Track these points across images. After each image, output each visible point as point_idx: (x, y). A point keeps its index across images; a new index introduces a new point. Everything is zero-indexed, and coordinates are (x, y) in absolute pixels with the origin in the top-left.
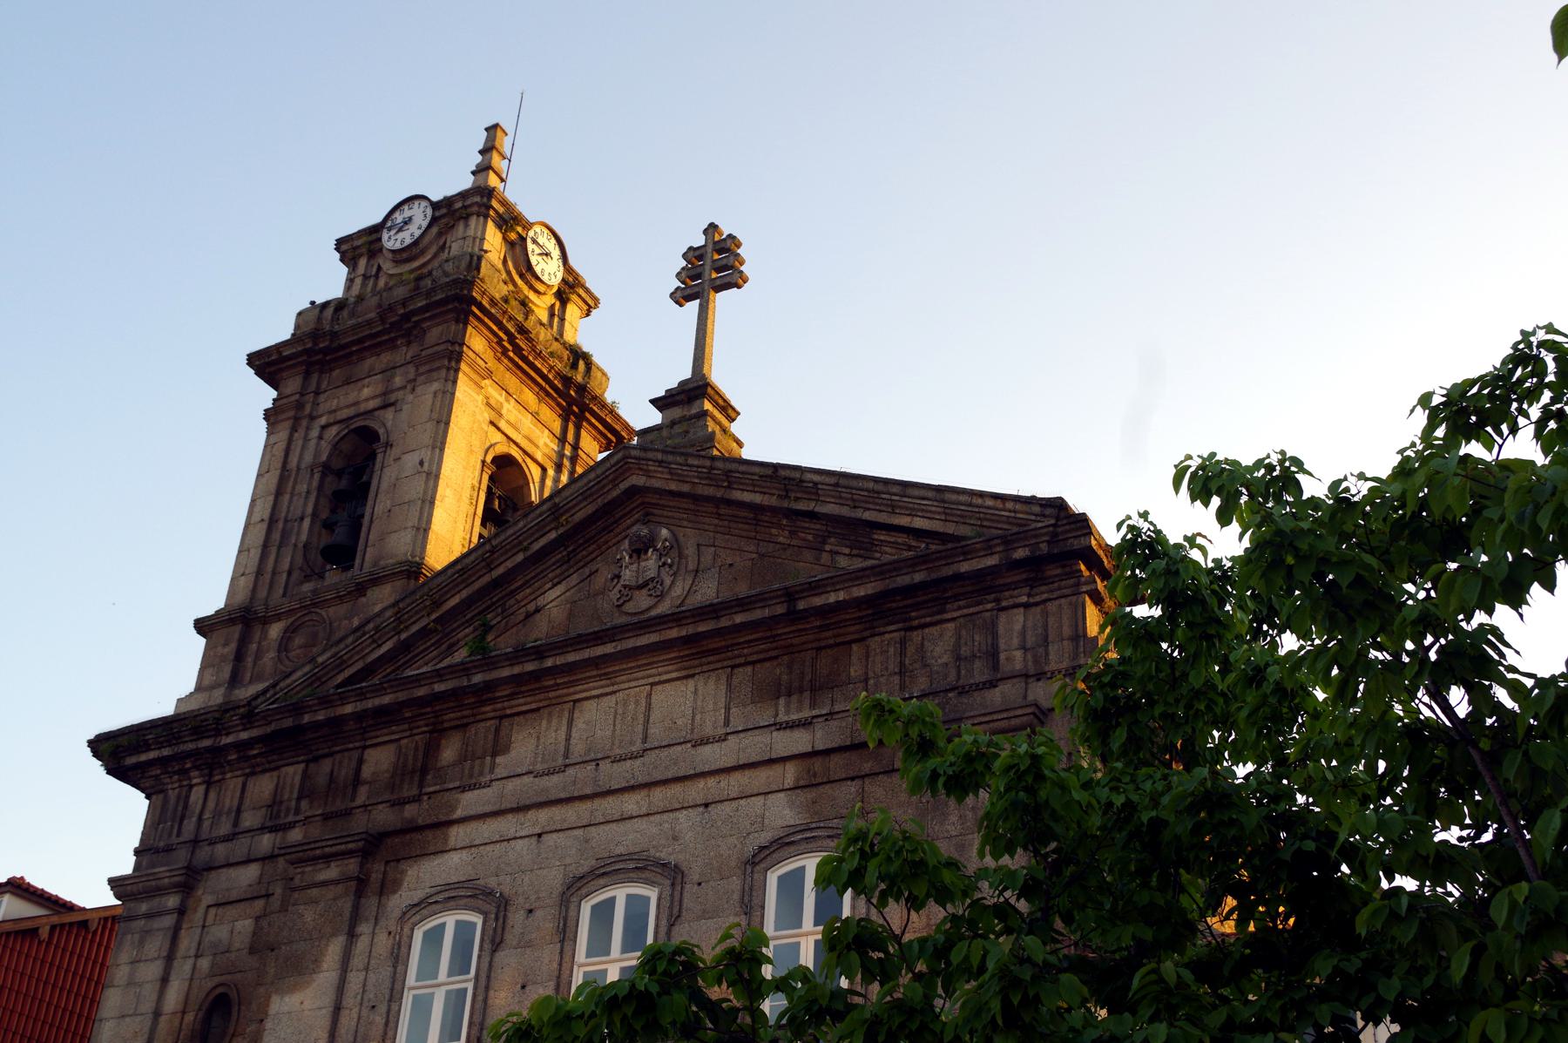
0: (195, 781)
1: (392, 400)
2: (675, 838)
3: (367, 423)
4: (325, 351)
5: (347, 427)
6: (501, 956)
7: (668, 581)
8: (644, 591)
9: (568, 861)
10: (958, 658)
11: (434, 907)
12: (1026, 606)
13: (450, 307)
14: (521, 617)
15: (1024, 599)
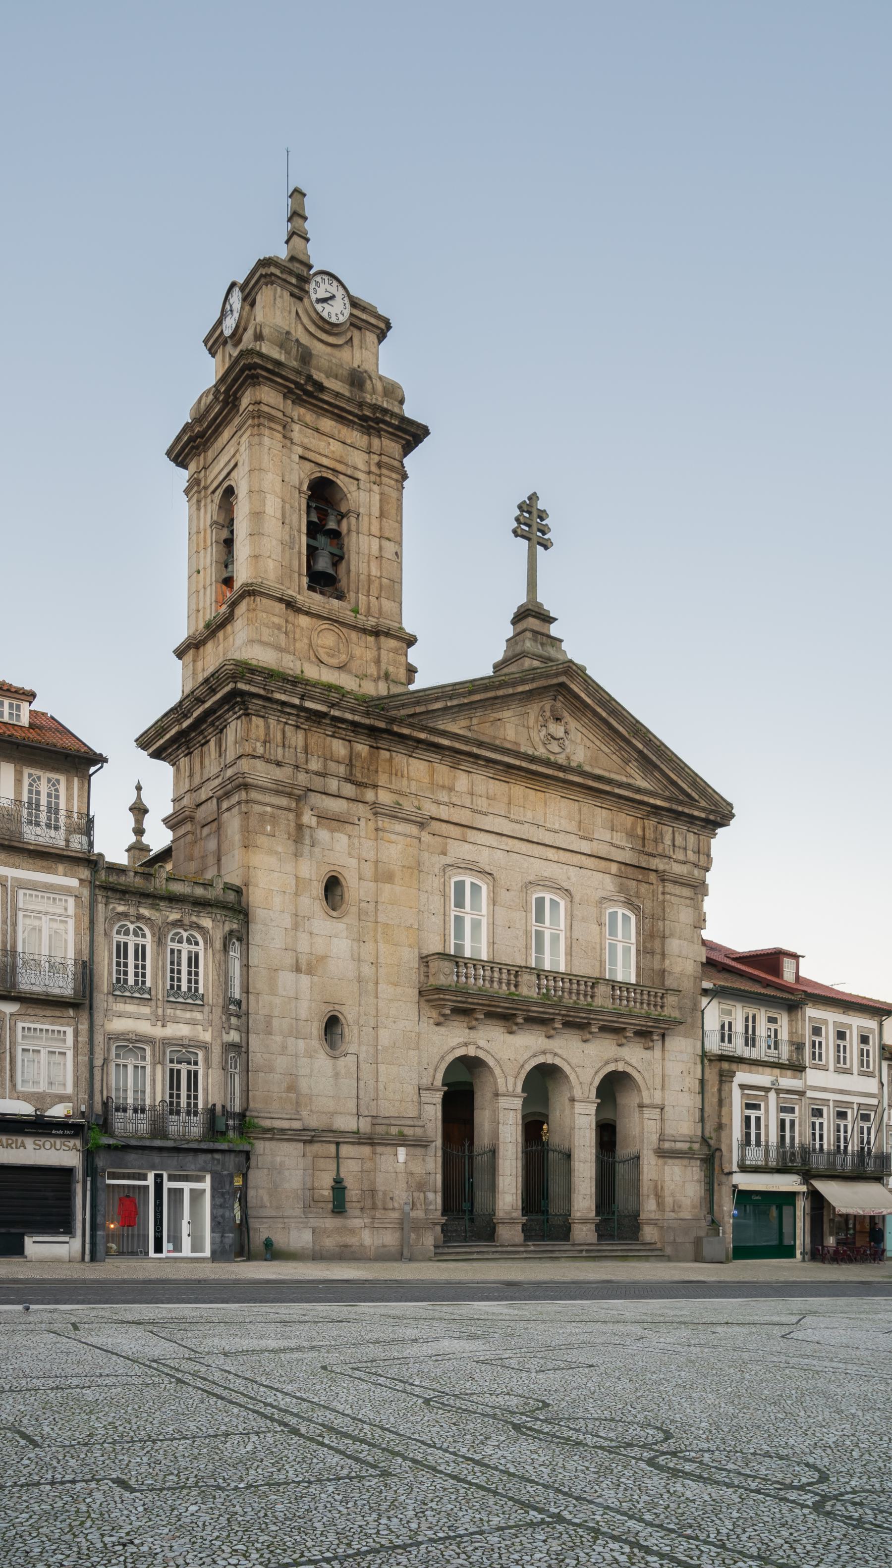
0: (290, 722)
1: (356, 476)
2: (569, 878)
3: (338, 482)
4: (306, 392)
5: (320, 472)
6: (497, 908)
7: (567, 742)
8: (556, 742)
9: (523, 870)
10: (674, 846)
11: (460, 870)
12: (695, 833)
13: (408, 437)
14: (492, 719)
15: (696, 831)
